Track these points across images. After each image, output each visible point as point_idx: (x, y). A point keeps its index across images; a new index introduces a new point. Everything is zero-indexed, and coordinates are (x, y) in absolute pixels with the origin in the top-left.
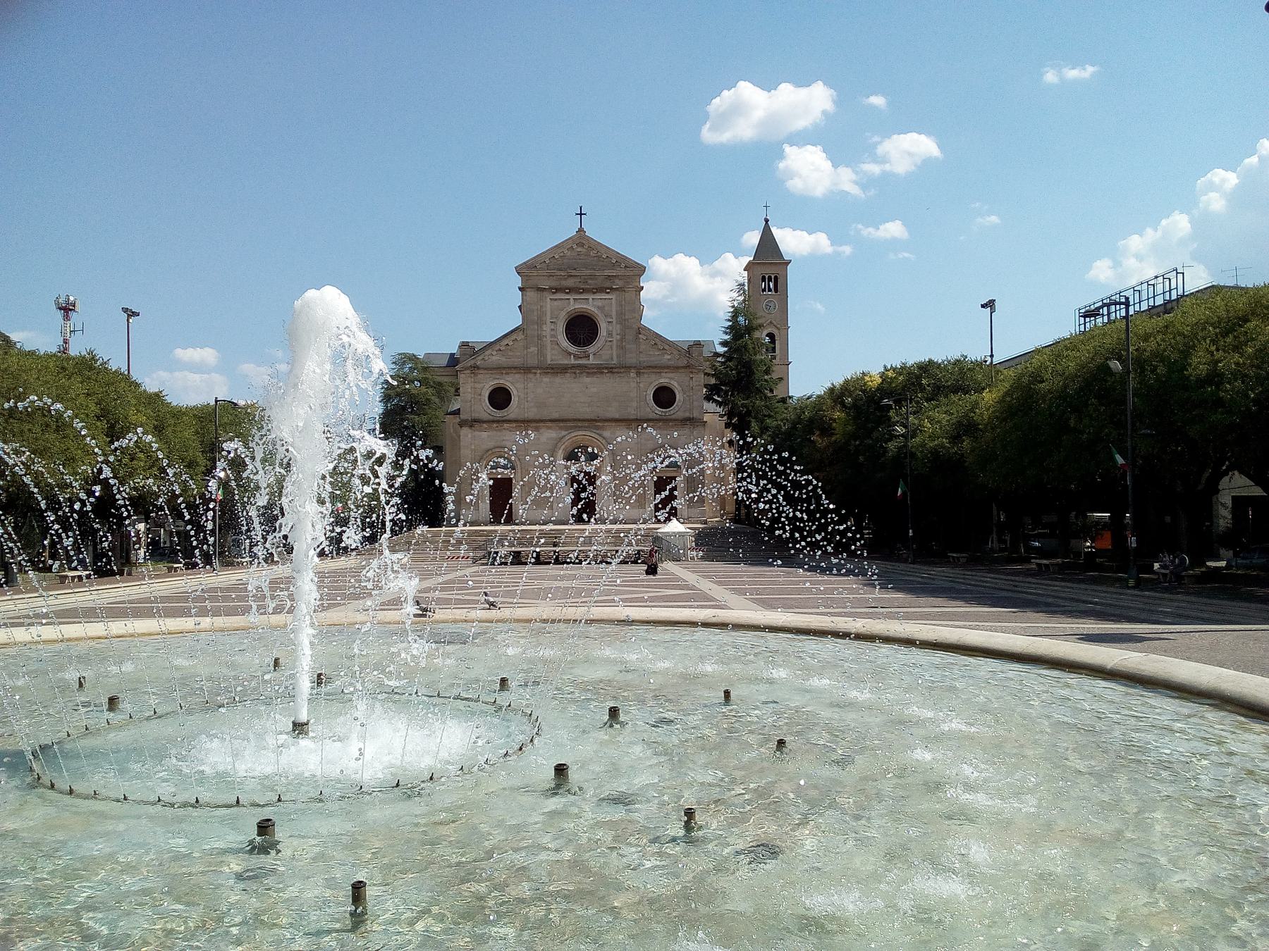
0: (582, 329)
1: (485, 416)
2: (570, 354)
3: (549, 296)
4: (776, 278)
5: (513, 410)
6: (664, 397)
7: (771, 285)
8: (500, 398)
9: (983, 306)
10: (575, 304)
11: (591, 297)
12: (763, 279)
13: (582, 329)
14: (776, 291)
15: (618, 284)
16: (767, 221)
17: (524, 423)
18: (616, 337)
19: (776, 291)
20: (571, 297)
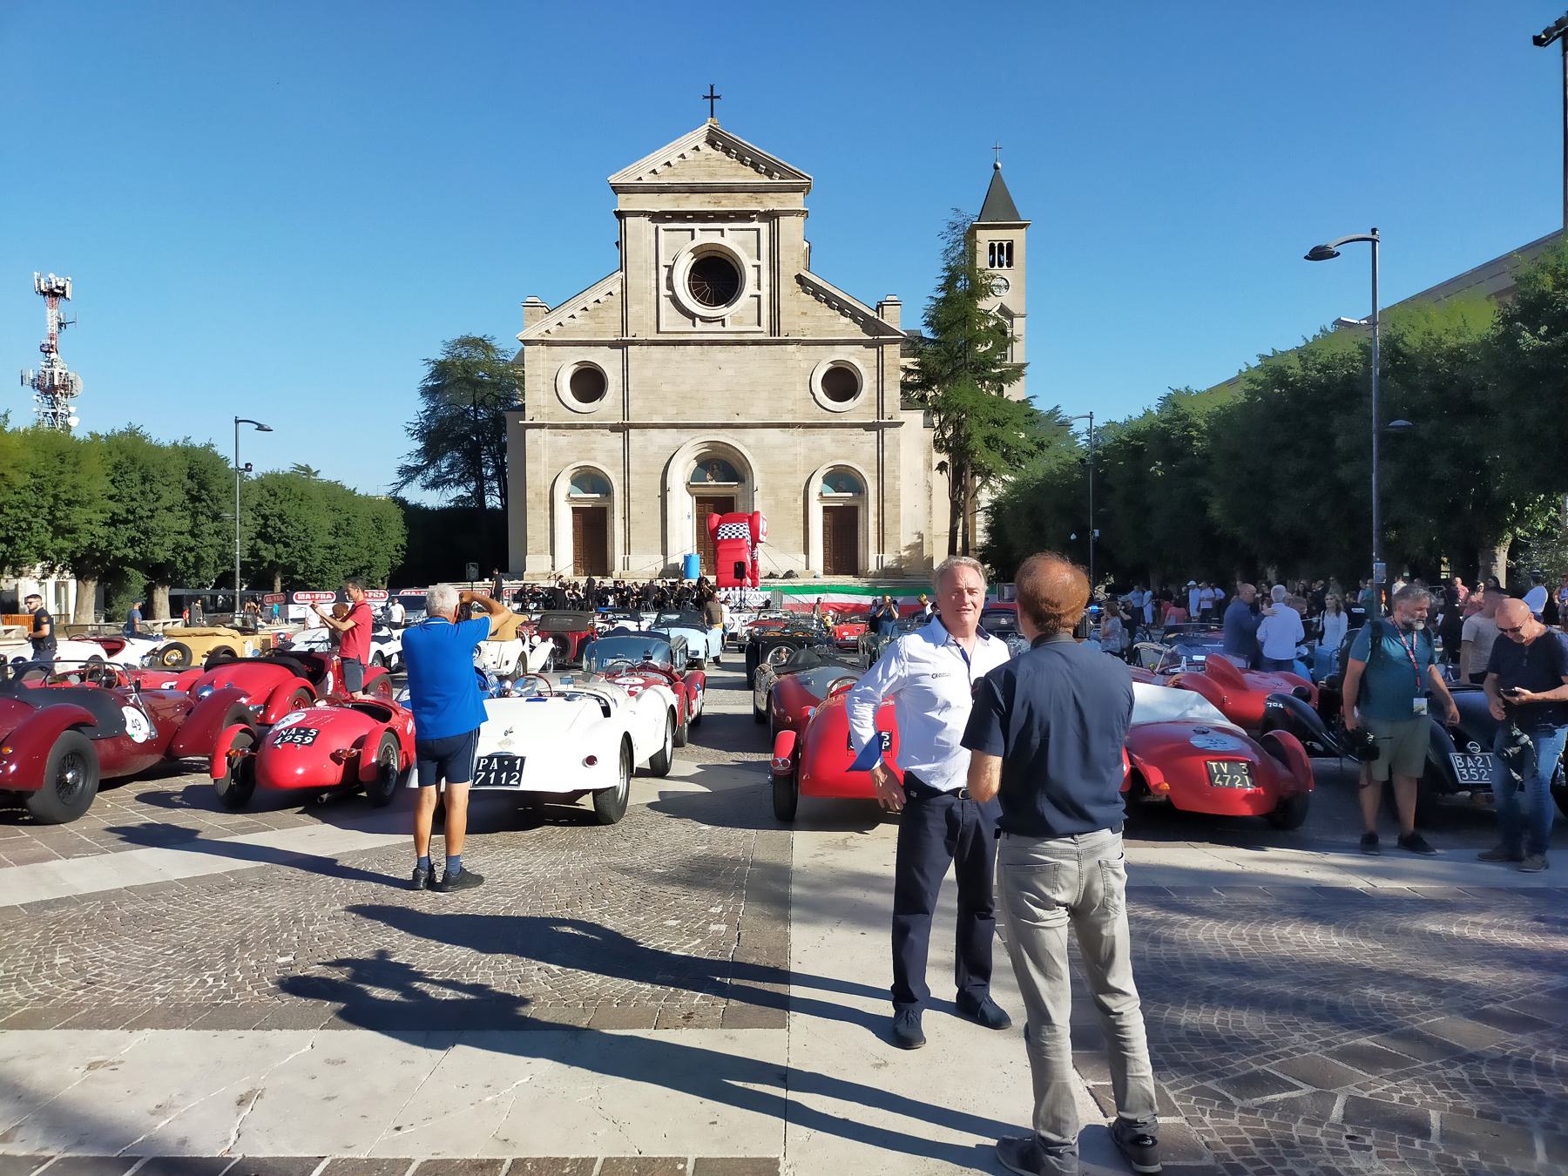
0: (716, 277)
1: (566, 417)
2: (692, 316)
3: (662, 226)
4: (1010, 246)
5: (607, 407)
6: (842, 383)
7: (1004, 258)
8: (589, 383)
9: (1538, 41)
10: (706, 236)
11: (726, 226)
12: (992, 247)
13: (716, 277)
14: (1009, 265)
15: (770, 203)
16: (996, 168)
17: (622, 428)
18: (765, 292)
19: (1009, 265)
20: (696, 226)
